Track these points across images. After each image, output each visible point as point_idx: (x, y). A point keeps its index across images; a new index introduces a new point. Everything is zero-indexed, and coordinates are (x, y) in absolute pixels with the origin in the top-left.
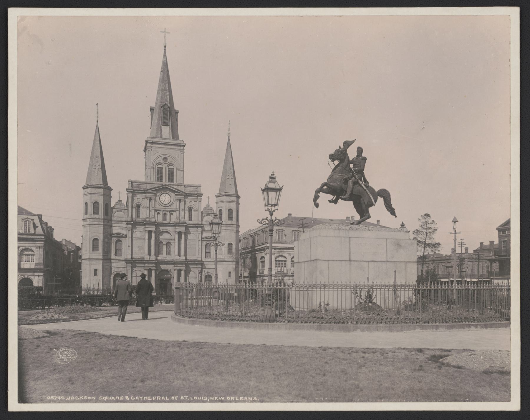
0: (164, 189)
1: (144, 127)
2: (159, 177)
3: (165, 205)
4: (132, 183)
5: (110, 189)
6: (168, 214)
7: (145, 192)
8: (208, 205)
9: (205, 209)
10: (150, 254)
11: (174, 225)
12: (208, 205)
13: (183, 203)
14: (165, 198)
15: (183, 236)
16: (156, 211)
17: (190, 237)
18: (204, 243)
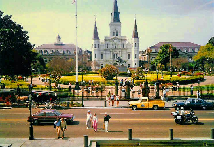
0: (115, 39)
1: (109, 19)
2: (113, 35)
3: (115, 43)
4: (105, 37)
5: (99, 39)
6: (116, 46)
7: (109, 40)
8: (129, 42)
9: (128, 43)
10: (111, 59)
11: (118, 49)
12: (129, 42)
13: (121, 42)
14: (115, 41)
15: (121, 53)
16: (112, 45)
17: (123, 52)
18: (128, 54)
